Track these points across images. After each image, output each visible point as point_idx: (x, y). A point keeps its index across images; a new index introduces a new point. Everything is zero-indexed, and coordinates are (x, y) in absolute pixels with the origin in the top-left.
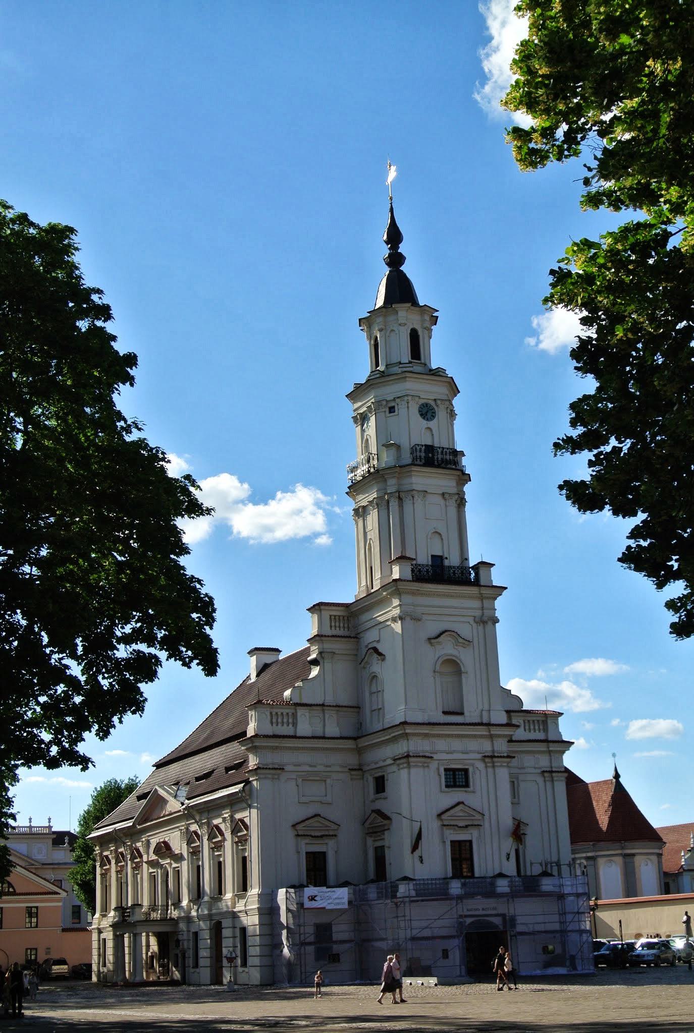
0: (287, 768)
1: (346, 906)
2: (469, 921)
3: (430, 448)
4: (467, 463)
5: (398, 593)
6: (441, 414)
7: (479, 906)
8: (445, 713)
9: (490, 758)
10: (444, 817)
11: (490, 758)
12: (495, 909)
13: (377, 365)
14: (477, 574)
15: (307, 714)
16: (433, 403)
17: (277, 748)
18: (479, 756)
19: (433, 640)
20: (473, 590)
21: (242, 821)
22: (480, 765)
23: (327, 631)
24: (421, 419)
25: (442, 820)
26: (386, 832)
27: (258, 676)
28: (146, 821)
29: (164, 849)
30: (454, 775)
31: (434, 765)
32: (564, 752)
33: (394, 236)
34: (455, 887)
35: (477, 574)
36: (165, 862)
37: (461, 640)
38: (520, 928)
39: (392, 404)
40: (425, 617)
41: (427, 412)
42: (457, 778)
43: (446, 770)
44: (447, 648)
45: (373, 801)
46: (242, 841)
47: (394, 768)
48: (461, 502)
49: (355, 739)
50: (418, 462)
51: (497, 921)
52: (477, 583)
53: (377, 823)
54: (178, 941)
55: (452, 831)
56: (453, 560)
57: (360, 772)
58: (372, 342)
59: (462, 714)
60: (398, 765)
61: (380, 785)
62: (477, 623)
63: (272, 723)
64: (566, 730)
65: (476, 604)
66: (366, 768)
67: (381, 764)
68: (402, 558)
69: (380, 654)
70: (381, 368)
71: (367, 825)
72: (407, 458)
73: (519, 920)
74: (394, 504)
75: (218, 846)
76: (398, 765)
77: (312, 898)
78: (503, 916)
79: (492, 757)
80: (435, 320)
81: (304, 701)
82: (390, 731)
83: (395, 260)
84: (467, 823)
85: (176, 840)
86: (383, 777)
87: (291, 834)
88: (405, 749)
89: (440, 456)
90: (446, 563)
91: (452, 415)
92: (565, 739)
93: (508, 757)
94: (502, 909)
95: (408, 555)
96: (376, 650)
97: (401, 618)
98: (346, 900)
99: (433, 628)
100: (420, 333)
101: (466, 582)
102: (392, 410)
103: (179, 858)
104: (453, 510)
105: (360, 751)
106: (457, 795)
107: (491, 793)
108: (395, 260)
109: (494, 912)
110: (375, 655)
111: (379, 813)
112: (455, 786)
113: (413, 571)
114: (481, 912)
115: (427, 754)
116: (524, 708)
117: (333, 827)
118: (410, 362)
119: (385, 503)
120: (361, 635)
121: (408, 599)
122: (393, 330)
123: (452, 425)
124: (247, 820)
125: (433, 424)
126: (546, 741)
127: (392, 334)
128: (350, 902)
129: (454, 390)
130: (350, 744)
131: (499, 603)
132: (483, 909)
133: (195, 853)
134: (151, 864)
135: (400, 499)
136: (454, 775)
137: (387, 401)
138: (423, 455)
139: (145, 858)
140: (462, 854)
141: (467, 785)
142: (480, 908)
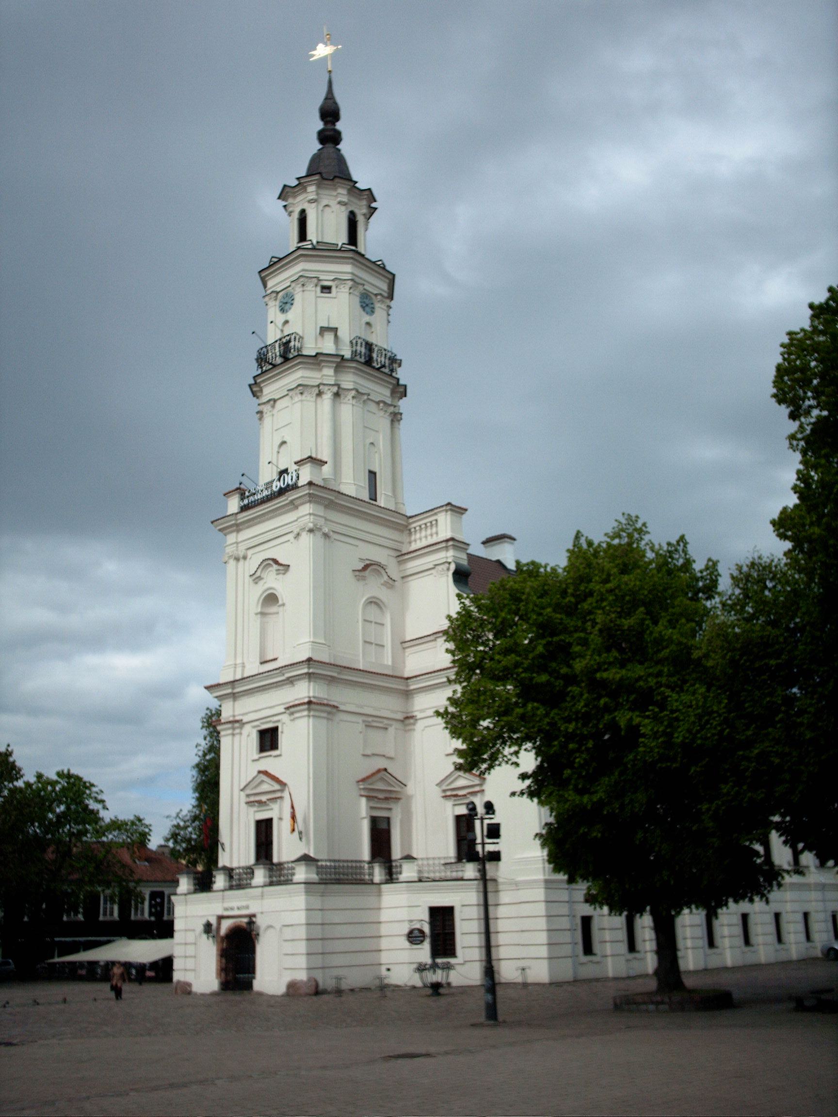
2: (226, 925)
8: (263, 663)
11: (291, 708)
12: (247, 907)
19: (256, 578)
22: (285, 718)
31: (247, 729)
33: (330, 113)
37: (275, 567)
40: (250, 552)
44: (272, 580)
55: (255, 809)
59: (275, 659)
83: (330, 138)
108: (330, 138)
115: (237, 718)
125: (290, 316)
132: (238, 908)
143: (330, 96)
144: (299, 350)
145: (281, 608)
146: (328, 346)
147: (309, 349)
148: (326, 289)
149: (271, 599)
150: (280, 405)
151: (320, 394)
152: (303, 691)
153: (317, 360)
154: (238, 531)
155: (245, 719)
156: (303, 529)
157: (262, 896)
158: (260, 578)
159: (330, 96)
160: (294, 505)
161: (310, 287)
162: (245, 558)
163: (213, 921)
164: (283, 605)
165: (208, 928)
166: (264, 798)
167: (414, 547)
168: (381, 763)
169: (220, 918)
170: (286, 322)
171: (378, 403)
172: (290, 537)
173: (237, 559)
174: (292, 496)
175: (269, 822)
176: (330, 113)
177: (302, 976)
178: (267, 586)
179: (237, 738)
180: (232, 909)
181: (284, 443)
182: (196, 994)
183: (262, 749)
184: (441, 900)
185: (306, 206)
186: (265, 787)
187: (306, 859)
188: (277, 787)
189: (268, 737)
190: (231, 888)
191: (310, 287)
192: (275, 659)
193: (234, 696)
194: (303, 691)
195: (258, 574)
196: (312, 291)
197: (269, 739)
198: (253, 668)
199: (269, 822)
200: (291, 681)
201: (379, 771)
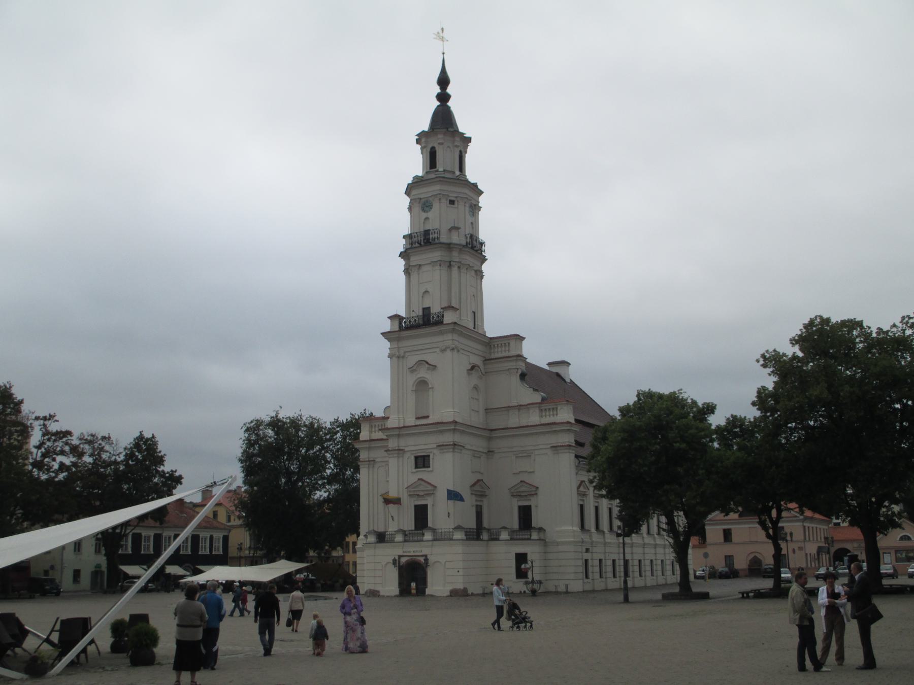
3: (427, 233)
7: (413, 550)
8: (418, 418)
18: (435, 446)
19: (412, 370)
22: (436, 451)
31: (407, 455)
33: (444, 81)
40: (407, 354)
42: (422, 461)
43: (416, 458)
44: (423, 373)
51: (422, 559)
59: (427, 417)
65: (440, 338)
78: (426, 556)
83: (443, 98)
94: (425, 551)
99: (412, 360)
106: (423, 474)
108: (443, 98)
114: (412, 554)
125: (430, 215)
140: (421, 513)
142: (411, 550)
143: (444, 71)
144: (438, 238)
146: (456, 239)
147: (444, 239)
148: (452, 202)
149: (422, 385)
150: (424, 268)
151: (450, 266)
152: (448, 438)
153: (449, 246)
154: (398, 341)
155: (406, 449)
156: (447, 348)
157: (432, 546)
158: (415, 370)
159: (444, 71)
160: (442, 333)
161: (444, 201)
162: (403, 357)
163: (397, 558)
165: (394, 561)
166: (421, 493)
167: (493, 356)
168: (479, 477)
169: (400, 557)
170: (427, 219)
171: (476, 271)
172: (438, 350)
173: (398, 357)
174: (442, 328)
175: (425, 507)
176: (444, 81)
177: (461, 587)
178: (419, 376)
179: (401, 459)
181: (426, 292)
182: (383, 596)
183: (417, 467)
184: (521, 550)
185: (436, 145)
186: (422, 488)
187: (458, 528)
188: (430, 488)
189: (420, 461)
190: (405, 541)
191: (444, 201)
192: (427, 417)
193: (399, 436)
194: (448, 438)
196: (445, 202)
197: (422, 461)
198: (411, 421)
199: (425, 507)
200: (441, 432)
201: (478, 481)
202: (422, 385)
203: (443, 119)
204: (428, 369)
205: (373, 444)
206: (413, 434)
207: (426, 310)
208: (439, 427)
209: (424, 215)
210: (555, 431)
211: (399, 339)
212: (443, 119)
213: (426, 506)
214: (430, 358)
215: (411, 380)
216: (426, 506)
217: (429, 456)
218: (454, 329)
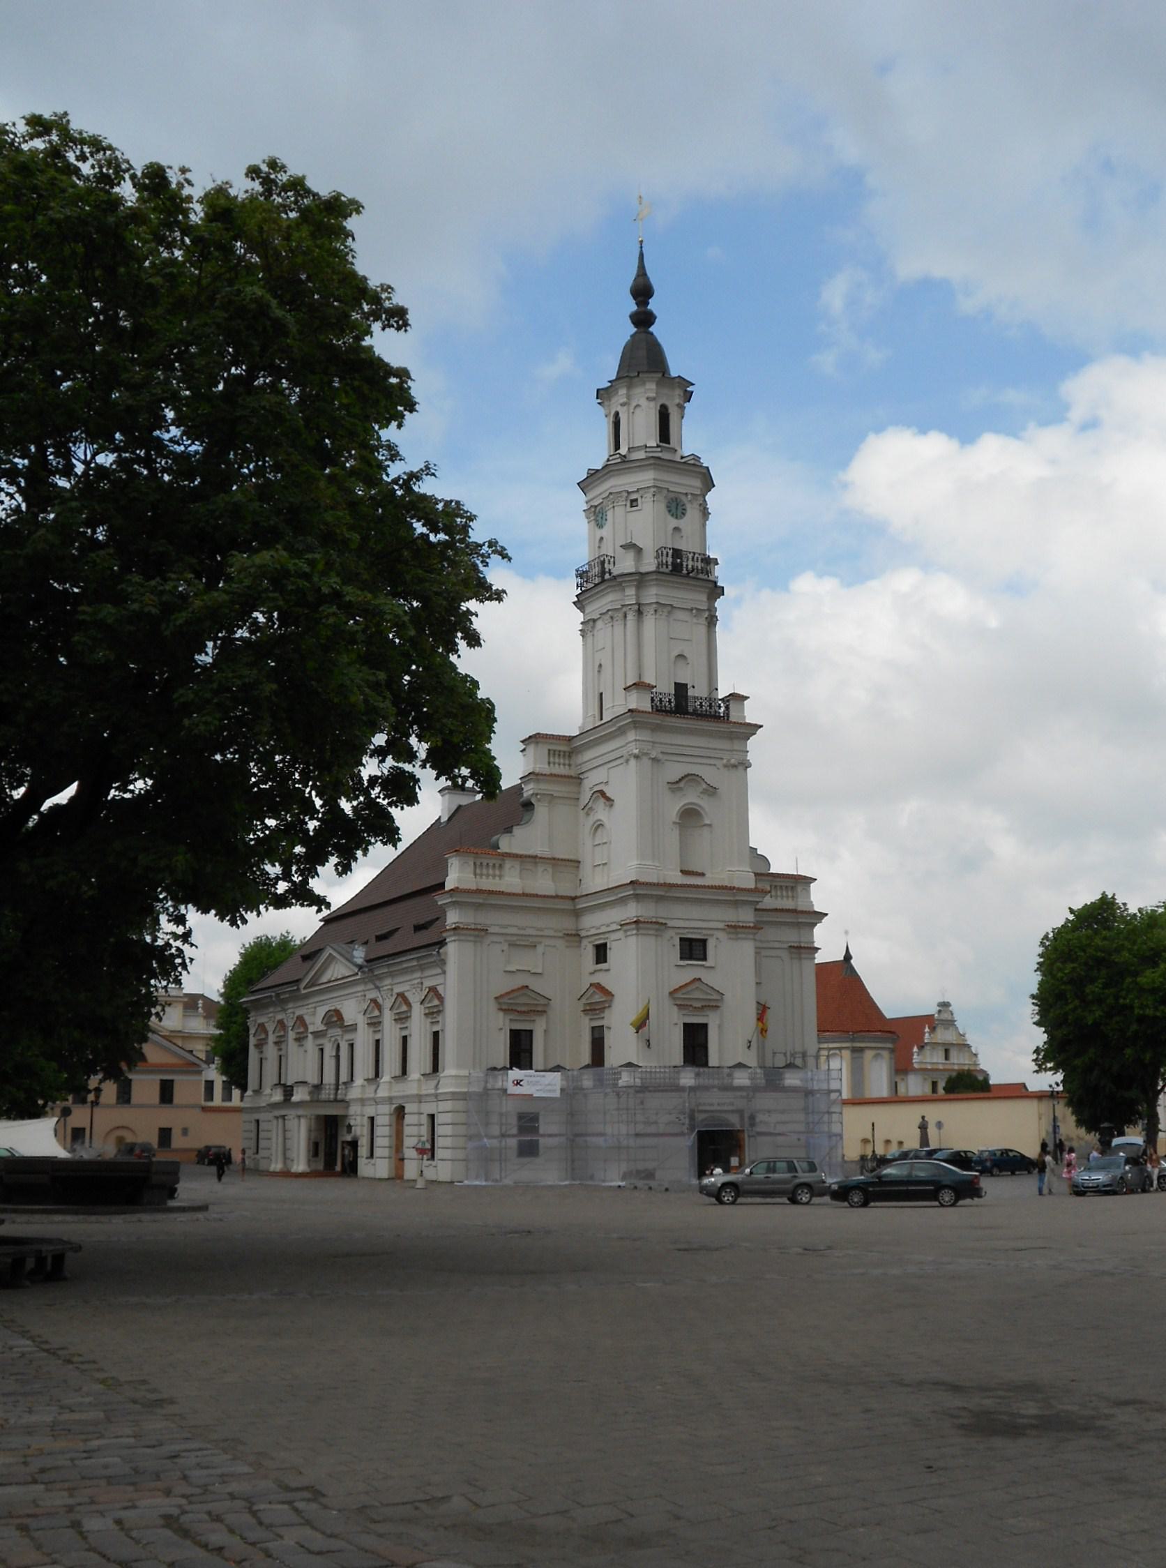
0: (491, 930)
1: (557, 1094)
3: (677, 553)
4: (720, 574)
5: (636, 725)
6: (692, 512)
8: (684, 872)
9: (734, 929)
10: (679, 995)
13: (617, 447)
14: (727, 708)
15: (518, 867)
16: (683, 498)
17: (481, 905)
18: (721, 925)
20: (722, 727)
21: (433, 990)
22: (721, 935)
23: (543, 767)
24: (669, 517)
25: (675, 999)
26: (607, 1011)
27: (450, 819)
28: (313, 985)
29: (335, 1019)
30: (690, 945)
32: (815, 924)
33: (642, 292)
34: (688, 1078)
35: (727, 708)
36: (336, 1032)
37: (704, 786)
38: (759, 1129)
39: (633, 497)
41: (676, 507)
42: (693, 949)
43: (681, 939)
44: (691, 797)
45: (592, 974)
46: (434, 1013)
47: (620, 934)
48: (712, 621)
49: (573, 899)
50: (664, 569)
52: (726, 718)
53: (598, 1001)
54: (349, 1127)
56: (698, 691)
57: (576, 939)
58: (612, 418)
59: (703, 875)
60: (626, 931)
61: (601, 953)
62: (725, 766)
63: (475, 874)
64: (818, 898)
66: (583, 934)
67: (604, 929)
68: (639, 686)
69: (608, 799)
70: (623, 450)
71: (584, 1000)
72: (649, 564)
73: (760, 1117)
74: (631, 617)
75: (402, 1018)
76: (626, 931)
77: (518, 1083)
78: (740, 1112)
79: (735, 927)
80: (688, 396)
81: (515, 851)
82: (616, 891)
83: (643, 319)
84: (704, 1003)
85: (352, 1010)
86: (605, 945)
87: (493, 1006)
88: (652, 913)
89: (690, 563)
90: (691, 692)
91: (705, 513)
92: (816, 909)
93: (754, 928)
95: (647, 681)
96: (602, 793)
97: (636, 757)
98: (558, 1088)
99: (675, 770)
100: (670, 411)
101: (716, 717)
102: (634, 503)
103: (353, 1028)
104: (702, 630)
105: (577, 914)
107: (733, 968)
108: (643, 319)
109: (730, 1108)
110: (602, 800)
111: (598, 987)
112: (691, 958)
113: (652, 700)
114: (716, 1108)
115: (661, 921)
116: (772, 871)
117: (545, 1002)
118: (658, 446)
119: (621, 615)
120: (585, 775)
121: (645, 735)
122: (638, 406)
123: (704, 526)
124: (440, 989)
125: (681, 523)
126: (795, 911)
127: (638, 410)
128: (562, 1090)
129: (709, 484)
130: (568, 905)
131: (752, 743)
133: (375, 1024)
134: (317, 1035)
135: (640, 612)
136: (690, 945)
137: (629, 493)
138: (670, 560)
139: (311, 1029)
141: (705, 959)
145: (706, 829)
155: (671, 923)
158: (680, 789)
164: (710, 825)
170: (677, 529)
176: (642, 292)
180: (712, 1105)
181: (681, 656)
192: (703, 875)
193: (660, 899)
195: (682, 784)
197: (693, 949)
200: (736, 904)
202: (690, 816)
203: (644, 359)
204: (705, 792)
205: (493, 900)
206: (687, 900)
207: (681, 689)
208: (729, 895)
209: (673, 522)
210: (799, 923)
211: (656, 728)
212: (644, 359)
213: (705, 1026)
214: (709, 774)
215: (673, 806)
216: (705, 1026)
217: (704, 942)
218: (634, 722)
